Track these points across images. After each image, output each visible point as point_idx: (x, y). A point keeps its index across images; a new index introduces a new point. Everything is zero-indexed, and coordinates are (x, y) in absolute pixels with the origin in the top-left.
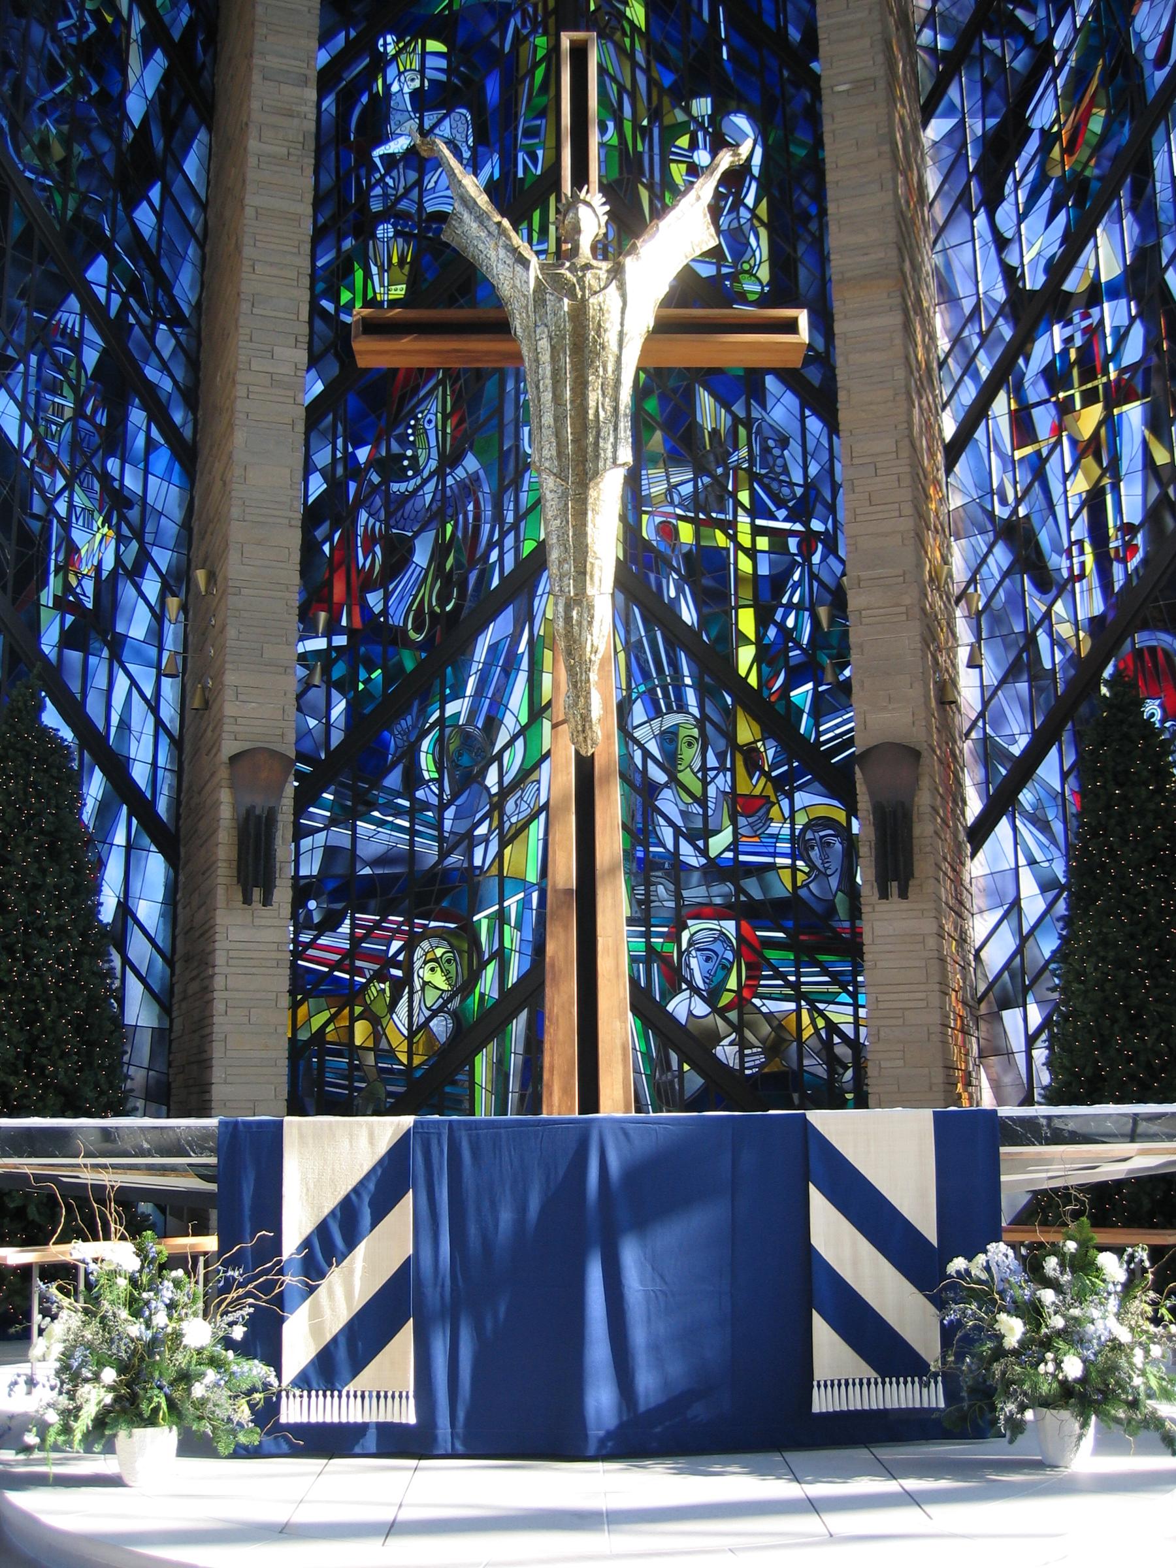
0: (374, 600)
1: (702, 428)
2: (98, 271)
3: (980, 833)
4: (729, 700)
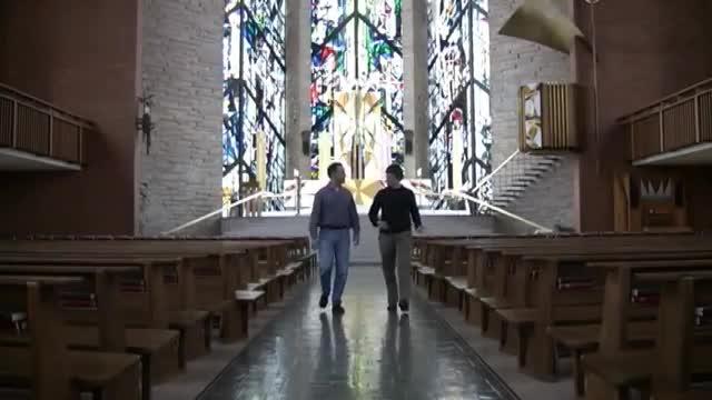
0: (320, 97)
2: (269, 38)
3: (431, 142)
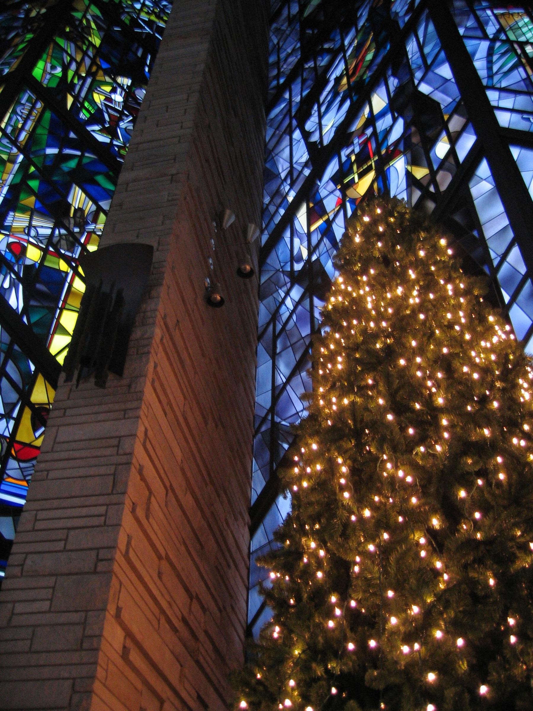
1: (70, 205)
4: (33, 368)
